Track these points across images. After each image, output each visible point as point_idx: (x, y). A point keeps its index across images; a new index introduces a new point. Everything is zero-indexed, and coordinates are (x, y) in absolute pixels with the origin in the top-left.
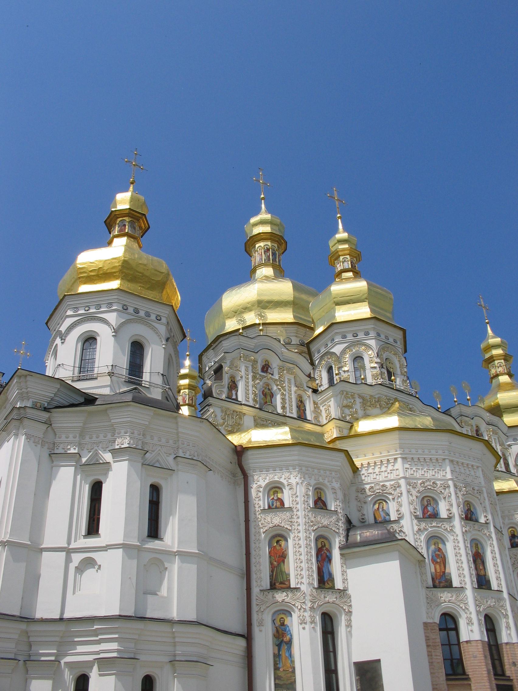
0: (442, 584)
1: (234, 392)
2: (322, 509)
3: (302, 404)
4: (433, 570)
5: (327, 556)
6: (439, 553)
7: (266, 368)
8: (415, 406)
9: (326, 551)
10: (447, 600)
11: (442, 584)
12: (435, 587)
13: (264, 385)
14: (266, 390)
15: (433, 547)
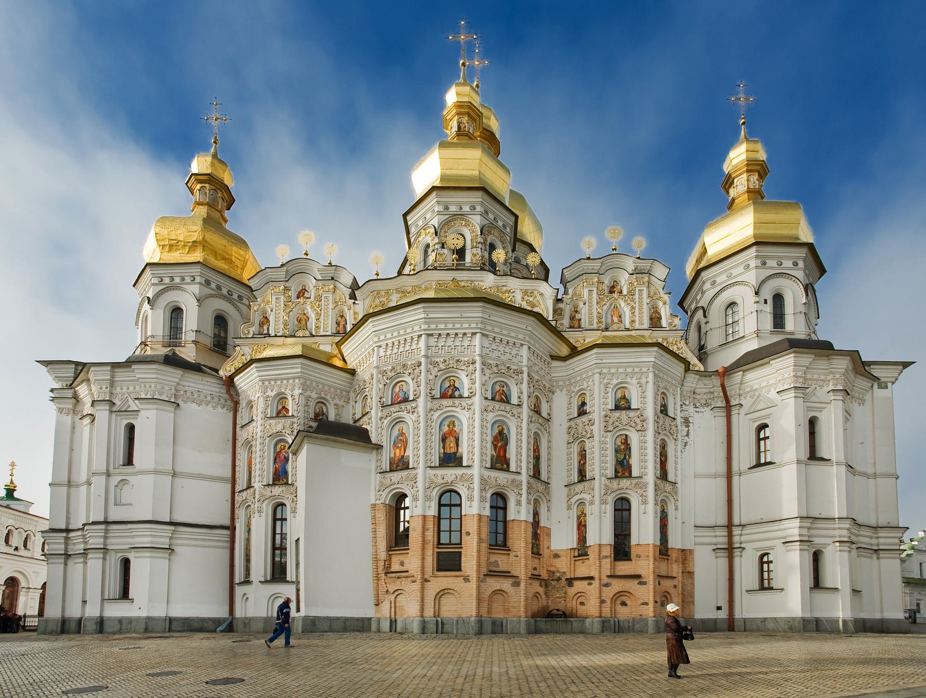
0: (399, 468)
1: (265, 327)
2: (285, 416)
3: (343, 319)
4: (393, 456)
5: (285, 457)
6: (401, 438)
7: (301, 293)
8: (481, 281)
9: (284, 454)
10: (396, 482)
11: (399, 468)
12: (391, 471)
13: (300, 312)
14: (302, 316)
15: (396, 432)
